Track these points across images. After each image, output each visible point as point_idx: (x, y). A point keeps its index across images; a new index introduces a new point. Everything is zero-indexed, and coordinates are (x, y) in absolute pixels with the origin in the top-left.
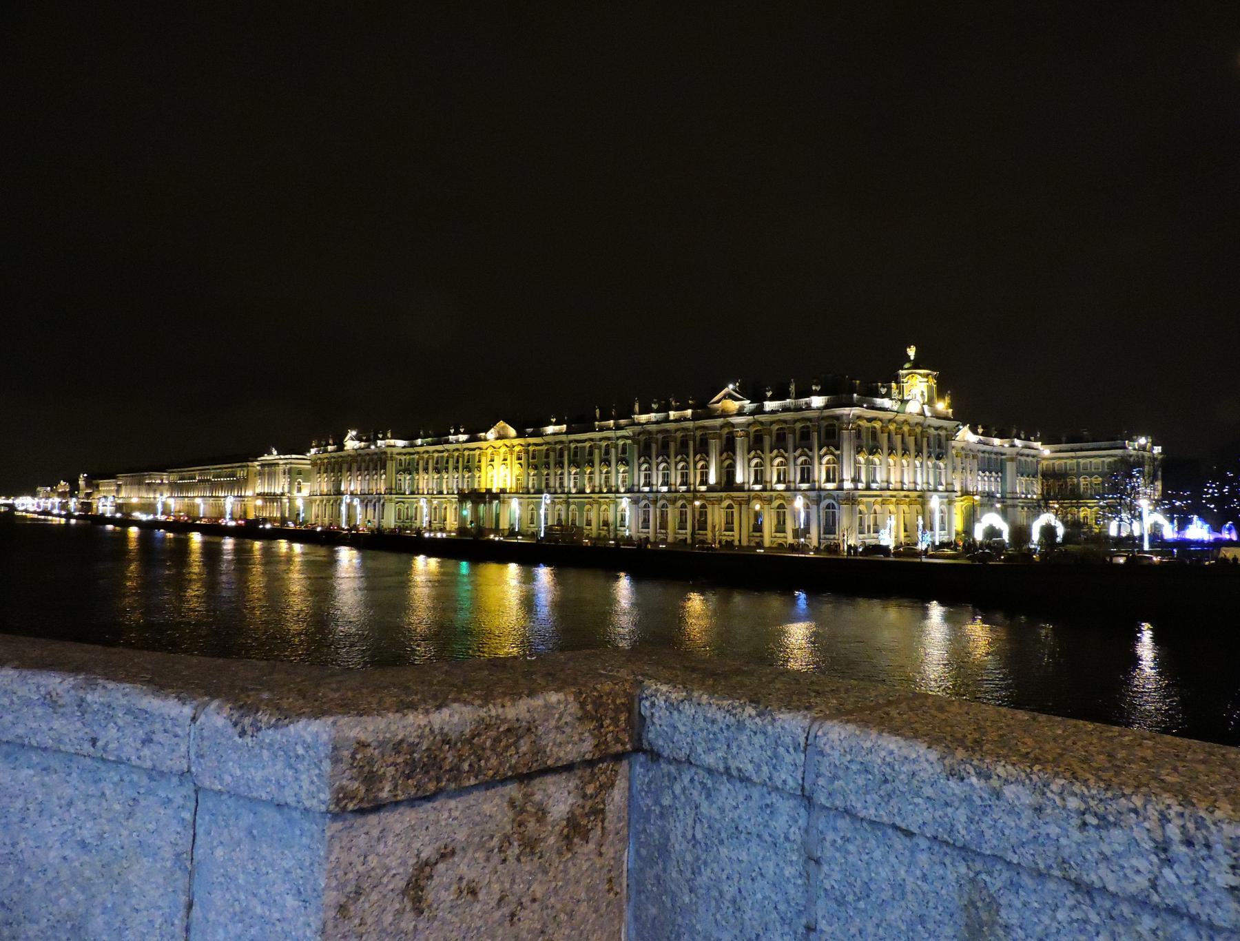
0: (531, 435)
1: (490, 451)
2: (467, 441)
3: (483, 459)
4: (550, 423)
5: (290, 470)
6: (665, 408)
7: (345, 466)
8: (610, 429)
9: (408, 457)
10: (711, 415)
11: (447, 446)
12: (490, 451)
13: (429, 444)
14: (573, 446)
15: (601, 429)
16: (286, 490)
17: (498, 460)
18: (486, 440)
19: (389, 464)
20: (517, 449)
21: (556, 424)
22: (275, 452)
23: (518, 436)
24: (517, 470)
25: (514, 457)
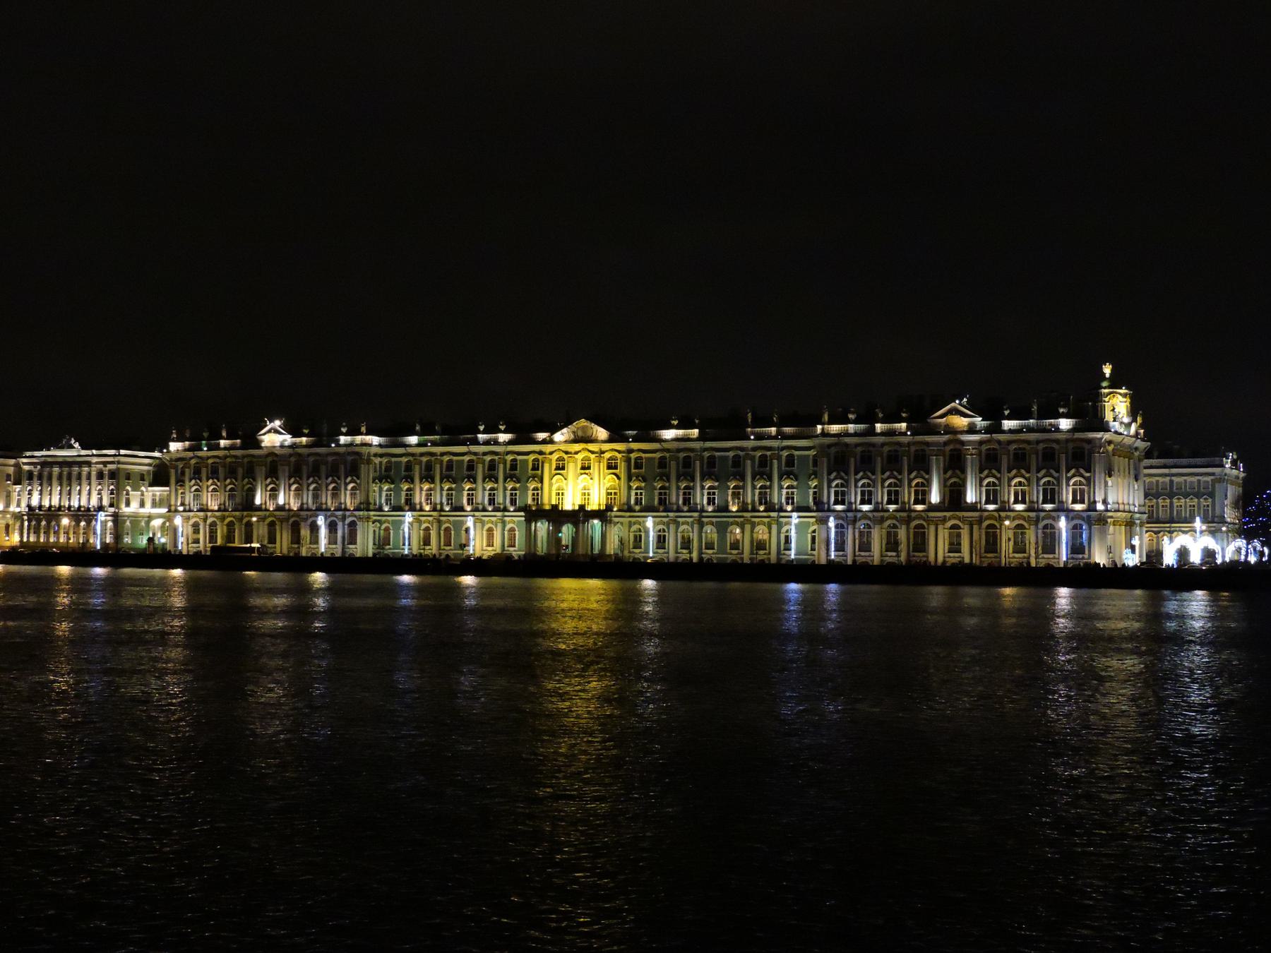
0: (636, 440)
1: (555, 456)
2: (510, 443)
3: (546, 466)
4: (670, 427)
5: (113, 475)
6: (868, 418)
7: (260, 472)
8: (770, 437)
9: (385, 460)
10: (934, 430)
11: (474, 448)
12: (555, 456)
13: (434, 444)
14: (706, 454)
15: (759, 437)
16: (106, 502)
17: (572, 469)
18: (551, 442)
19: (363, 468)
20: (607, 455)
21: (677, 427)
22: (77, 445)
23: (610, 440)
24: (609, 480)
25: (604, 465)
